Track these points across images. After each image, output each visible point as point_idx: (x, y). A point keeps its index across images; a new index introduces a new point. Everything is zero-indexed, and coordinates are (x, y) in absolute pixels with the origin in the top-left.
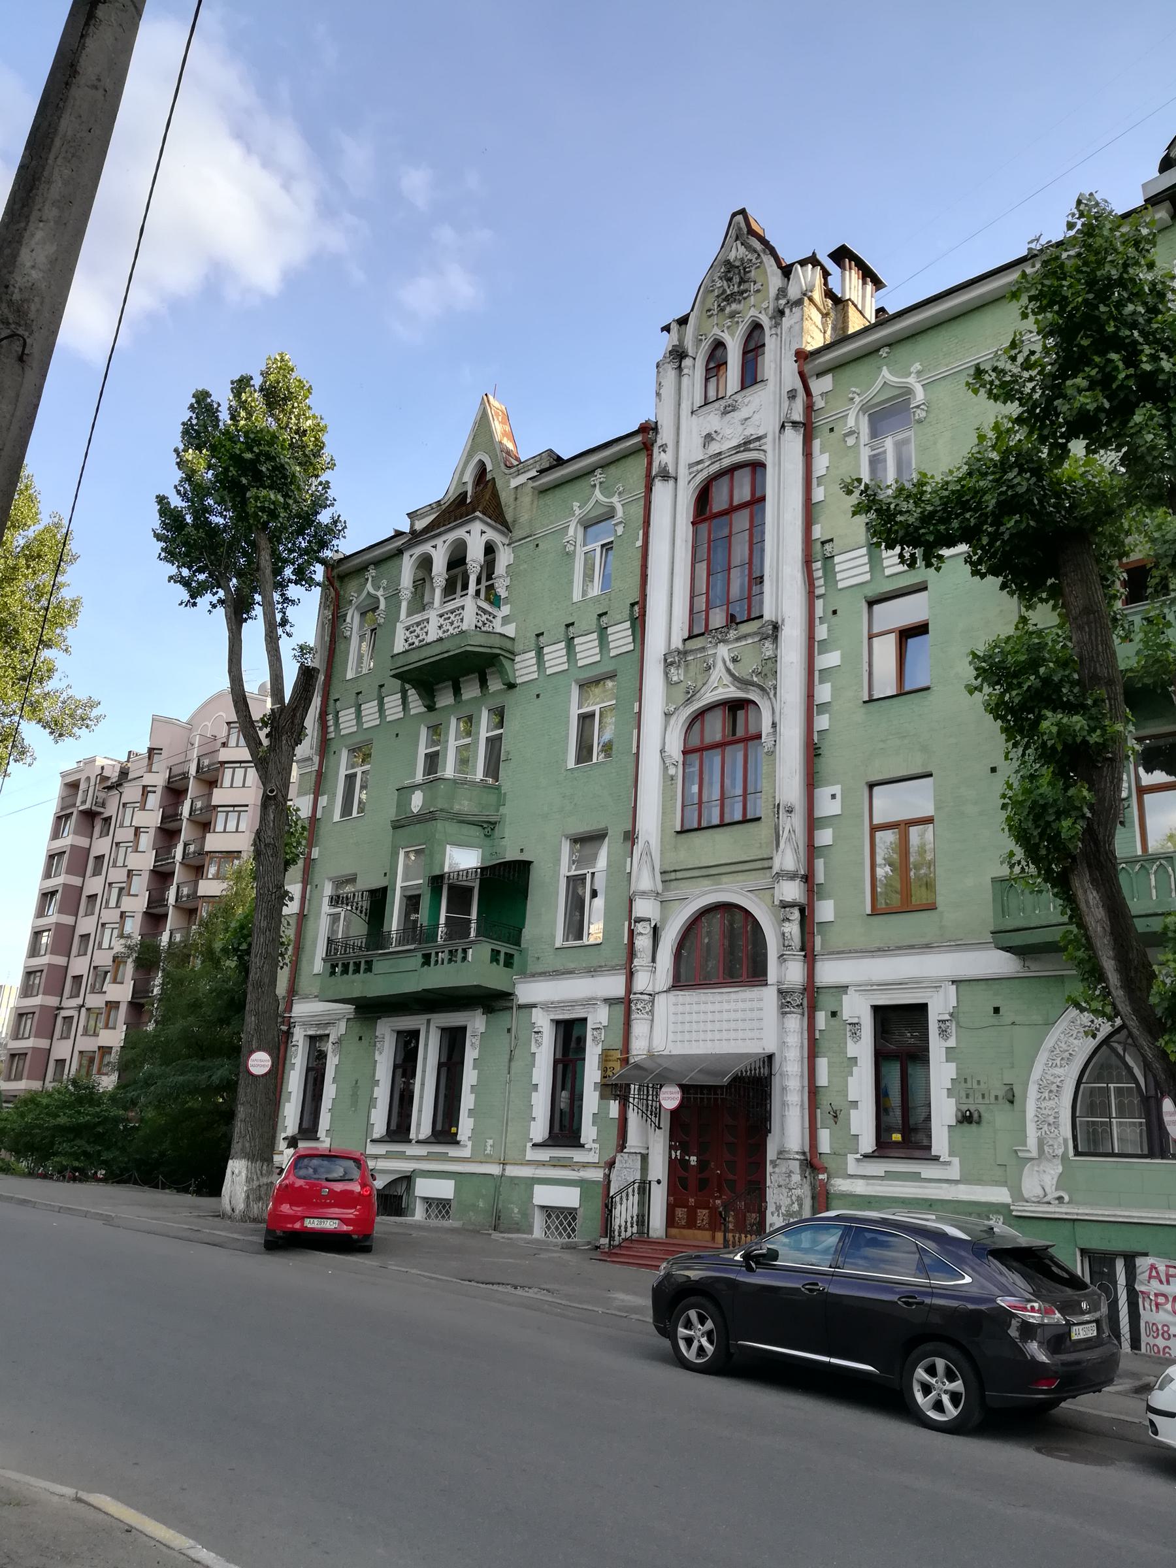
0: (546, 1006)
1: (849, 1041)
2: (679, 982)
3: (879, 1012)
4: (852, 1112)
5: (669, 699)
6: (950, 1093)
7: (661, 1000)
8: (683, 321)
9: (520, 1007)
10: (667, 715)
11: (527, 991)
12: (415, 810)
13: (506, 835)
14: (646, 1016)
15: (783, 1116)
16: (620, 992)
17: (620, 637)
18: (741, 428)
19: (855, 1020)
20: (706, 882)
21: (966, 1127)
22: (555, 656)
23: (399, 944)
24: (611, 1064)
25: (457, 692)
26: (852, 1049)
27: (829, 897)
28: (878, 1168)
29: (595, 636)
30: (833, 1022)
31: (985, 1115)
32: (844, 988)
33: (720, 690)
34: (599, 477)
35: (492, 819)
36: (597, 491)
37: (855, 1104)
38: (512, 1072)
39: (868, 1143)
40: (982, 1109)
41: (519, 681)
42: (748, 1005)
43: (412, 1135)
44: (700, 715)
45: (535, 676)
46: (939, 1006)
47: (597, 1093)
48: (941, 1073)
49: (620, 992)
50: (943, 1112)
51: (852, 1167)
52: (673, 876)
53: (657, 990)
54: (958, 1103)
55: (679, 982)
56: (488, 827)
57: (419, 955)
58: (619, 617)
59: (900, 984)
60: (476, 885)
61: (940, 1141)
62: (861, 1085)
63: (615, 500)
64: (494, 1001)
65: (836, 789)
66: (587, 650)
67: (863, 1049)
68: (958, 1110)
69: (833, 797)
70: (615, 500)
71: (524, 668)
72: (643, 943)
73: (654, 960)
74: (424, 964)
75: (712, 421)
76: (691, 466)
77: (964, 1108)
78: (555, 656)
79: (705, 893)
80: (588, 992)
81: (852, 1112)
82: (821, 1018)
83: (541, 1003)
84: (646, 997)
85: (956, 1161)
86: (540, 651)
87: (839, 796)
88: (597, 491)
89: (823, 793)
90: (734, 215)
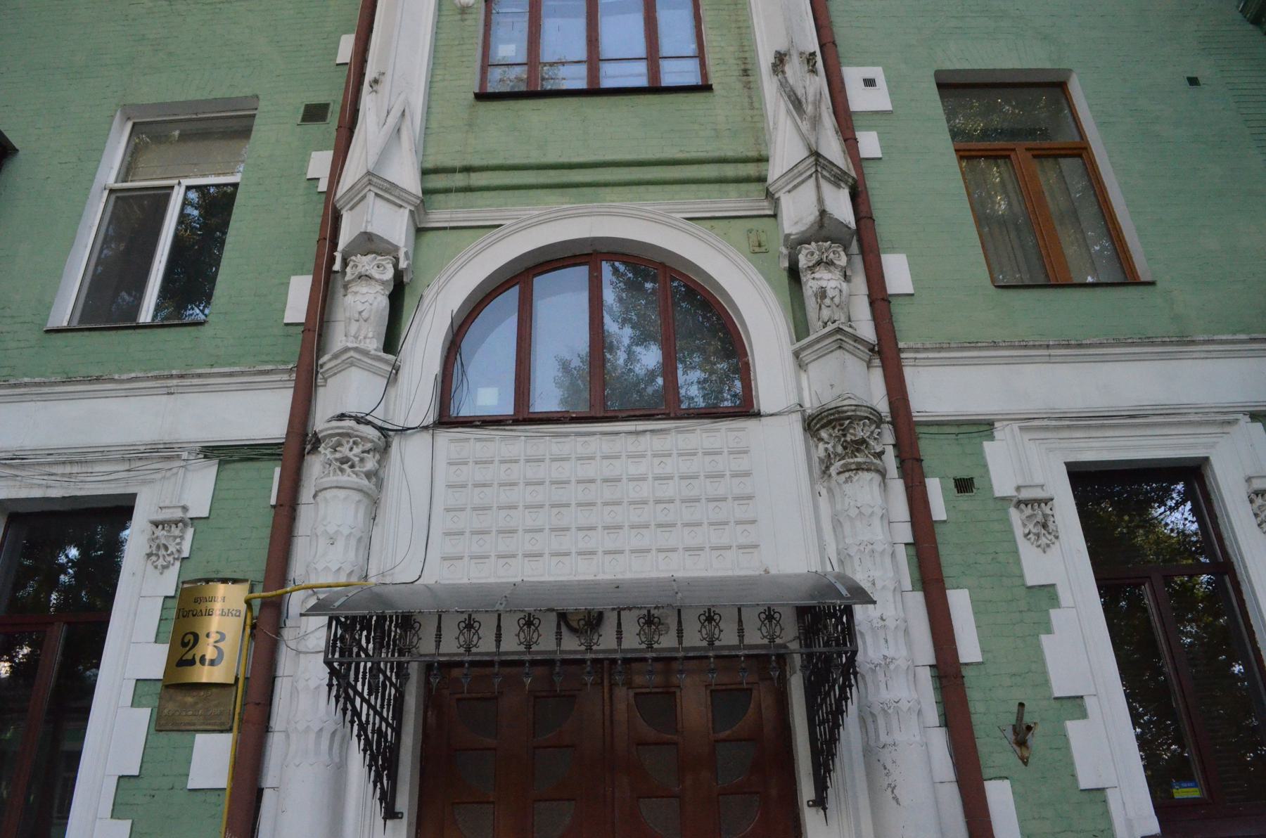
1: (1027, 552)
3: (1084, 478)
14: (364, 482)
15: (870, 752)
19: (1039, 494)
20: (551, 197)
26: (1037, 566)
27: (892, 250)
30: (964, 501)
32: (985, 427)
37: (1075, 705)
42: (694, 465)
47: (143, 715)
52: (459, 180)
53: (400, 422)
59: (1133, 418)
69: (869, 83)
72: (363, 304)
73: (391, 343)
82: (935, 488)
84: (372, 433)
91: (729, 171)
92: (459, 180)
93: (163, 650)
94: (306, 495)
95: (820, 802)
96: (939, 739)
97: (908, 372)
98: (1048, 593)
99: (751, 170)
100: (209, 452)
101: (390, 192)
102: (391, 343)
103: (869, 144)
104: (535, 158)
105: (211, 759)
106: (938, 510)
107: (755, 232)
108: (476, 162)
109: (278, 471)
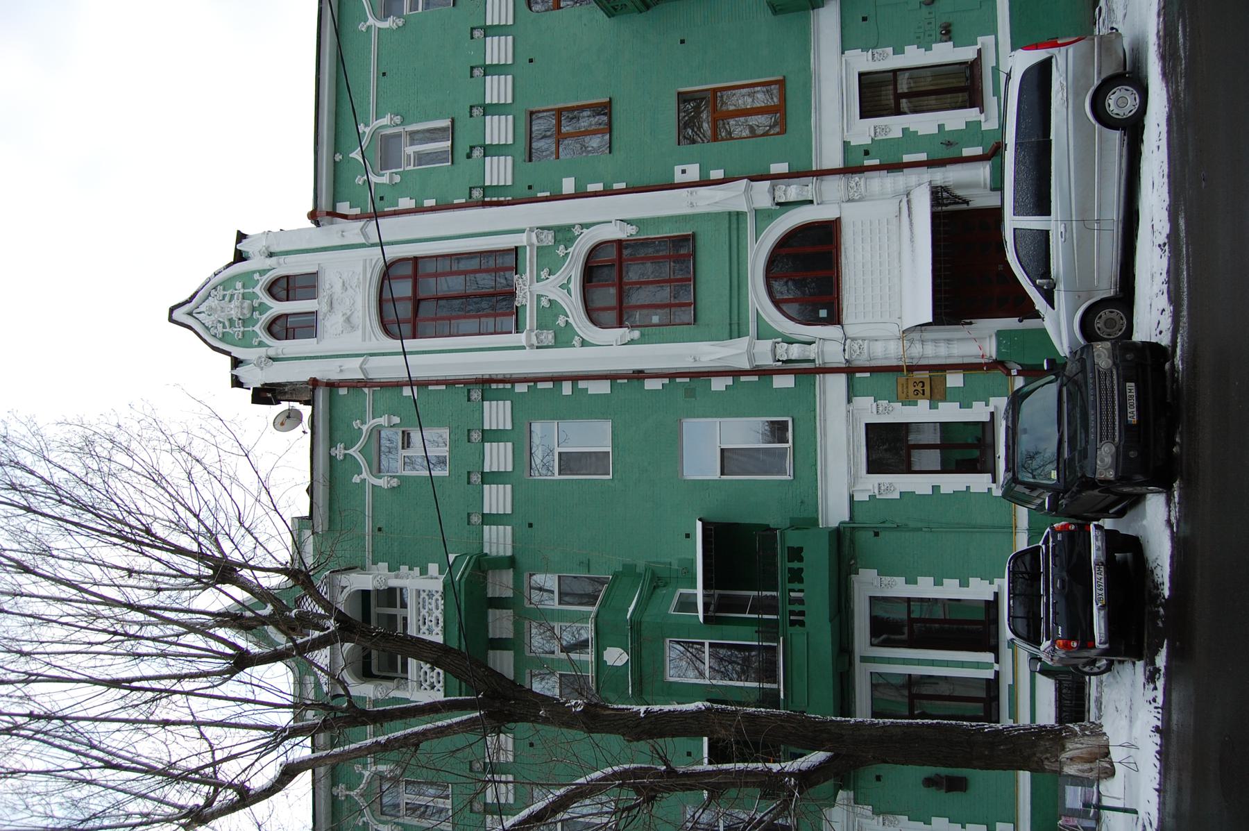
0: (853, 479)
2: (835, 318)
4: (947, 129)
5: (568, 344)
6: (929, 49)
7: (851, 331)
8: (236, 363)
9: (851, 518)
10: (584, 343)
11: (835, 512)
12: (625, 657)
13: (668, 560)
16: (842, 378)
17: (497, 414)
18: (350, 291)
21: (953, 34)
22: (497, 499)
23: (775, 681)
24: (912, 389)
25: (500, 644)
26: (897, 134)
28: (991, 101)
29: (487, 445)
31: (945, 20)
32: (846, 144)
33: (571, 286)
34: (339, 452)
35: (649, 576)
36: (350, 452)
37: (941, 127)
38: (920, 525)
39: (972, 114)
40: (938, 24)
41: (509, 553)
43: (989, 674)
44: (592, 313)
45: (509, 528)
46: (863, 61)
48: (914, 57)
49: (842, 378)
50: (945, 53)
51: (990, 124)
52: (735, 327)
54: (936, 42)
55: (835, 318)
56: (657, 581)
57: (791, 630)
58: (477, 415)
60: (718, 592)
61: (968, 54)
62: (925, 123)
63: (365, 428)
64: (845, 548)
65: (678, 169)
66: (498, 457)
67: (894, 126)
68: (941, 41)
69: (684, 172)
70: (365, 428)
71: (498, 540)
72: (795, 351)
74: (802, 623)
75: (331, 325)
76: (364, 340)
77: (939, 36)
78: (497, 499)
79: (754, 286)
80: (841, 422)
81: (947, 129)
82: (867, 163)
83: (849, 488)
84: (848, 341)
85: (980, 39)
86: (488, 519)
87: (683, 167)
88: (350, 452)
89: (679, 178)
90: (171, 320)
91: (734, 226)
92: (735, 327)
93: (920, 402)
94: (867, 364)
95: (967, 203)
96: (949, 167)
97: (824, 167)
98: (905, 130)
99: (734, 219)
100: (849, 401)
101: (751, 346)
102: (810, 343)
103: (717, 174)
104: (727, 298)
105: (954, 380)
106: (876, 162)
107: (764, 217)
108: (728, 321)
109: (858, 375)
